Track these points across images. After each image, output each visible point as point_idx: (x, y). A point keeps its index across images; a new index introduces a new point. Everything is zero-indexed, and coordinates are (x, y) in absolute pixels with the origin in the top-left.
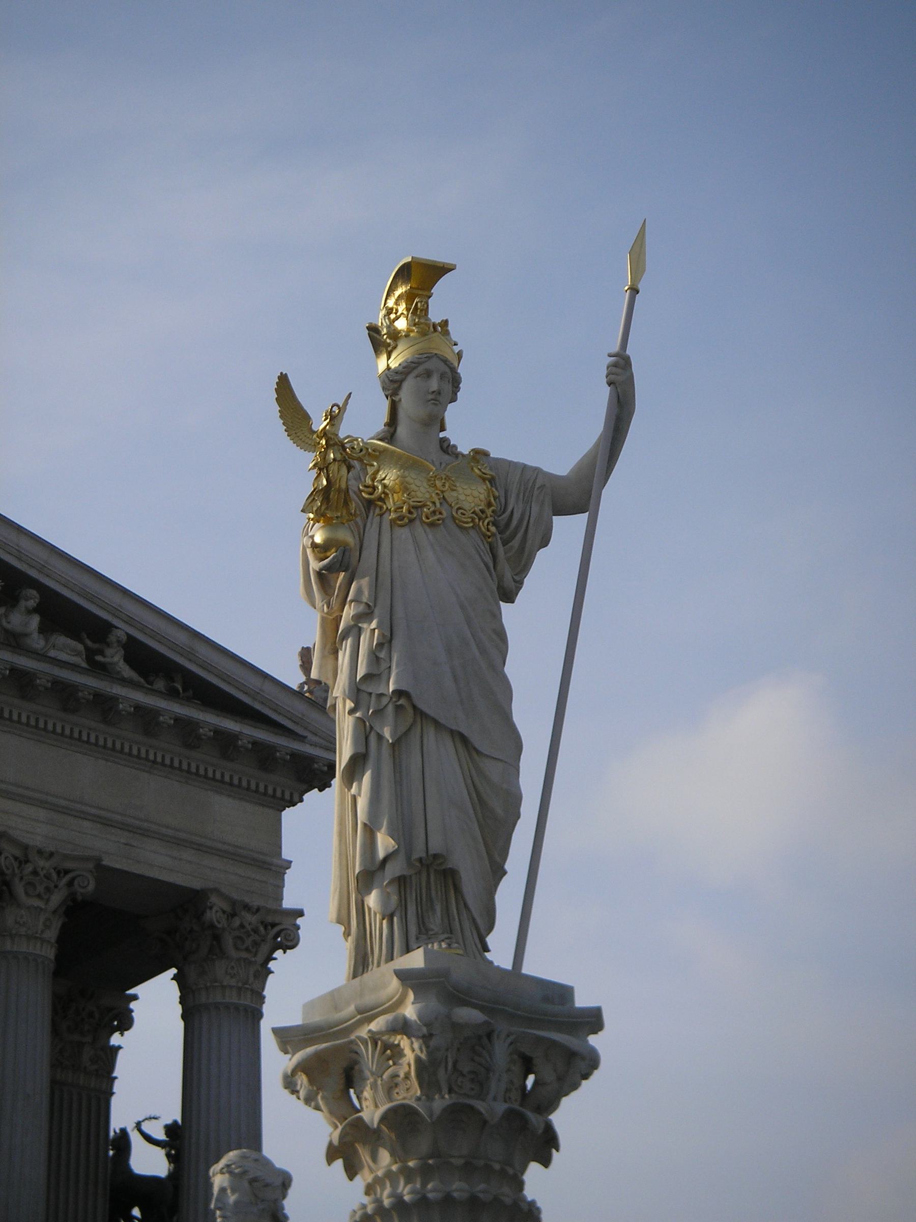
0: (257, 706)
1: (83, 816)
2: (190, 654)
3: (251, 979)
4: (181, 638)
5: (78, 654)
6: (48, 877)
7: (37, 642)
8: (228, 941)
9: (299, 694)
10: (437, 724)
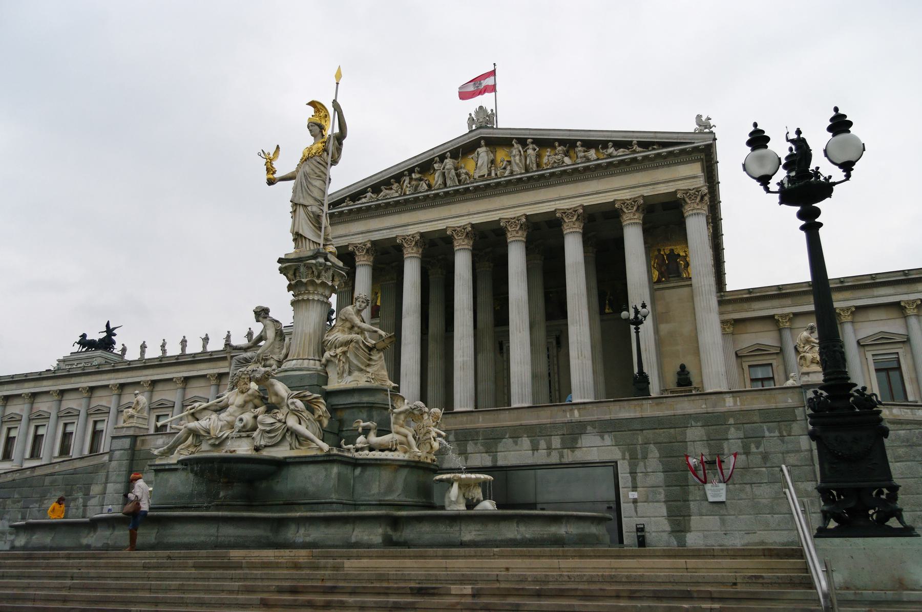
0: (679, 141)
1: (640, 186)
2: (656, 138)
3: (695, 206)
4: (652, 135)
5: (624, 152)
6: (631, 204)
7: (615, 153)
8: (687, 200)
9: (694, 133)
10: (300, 205)
